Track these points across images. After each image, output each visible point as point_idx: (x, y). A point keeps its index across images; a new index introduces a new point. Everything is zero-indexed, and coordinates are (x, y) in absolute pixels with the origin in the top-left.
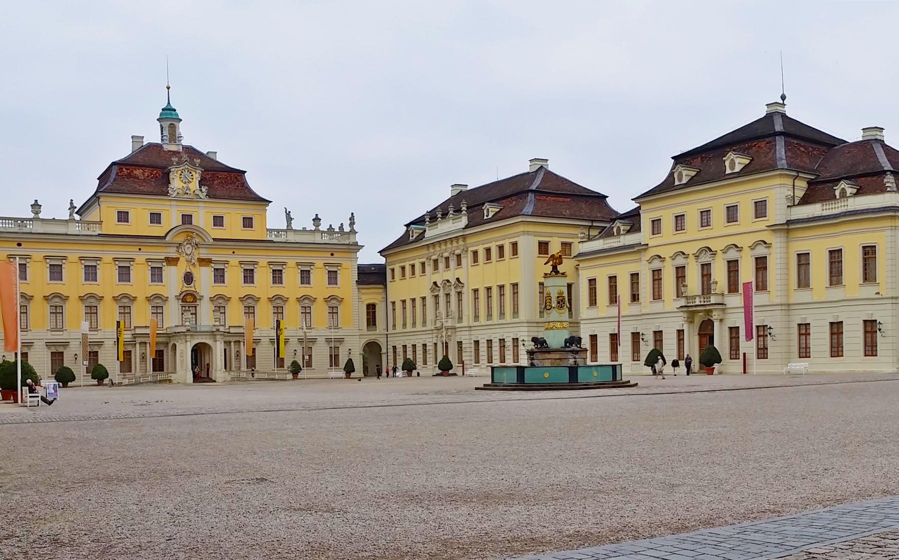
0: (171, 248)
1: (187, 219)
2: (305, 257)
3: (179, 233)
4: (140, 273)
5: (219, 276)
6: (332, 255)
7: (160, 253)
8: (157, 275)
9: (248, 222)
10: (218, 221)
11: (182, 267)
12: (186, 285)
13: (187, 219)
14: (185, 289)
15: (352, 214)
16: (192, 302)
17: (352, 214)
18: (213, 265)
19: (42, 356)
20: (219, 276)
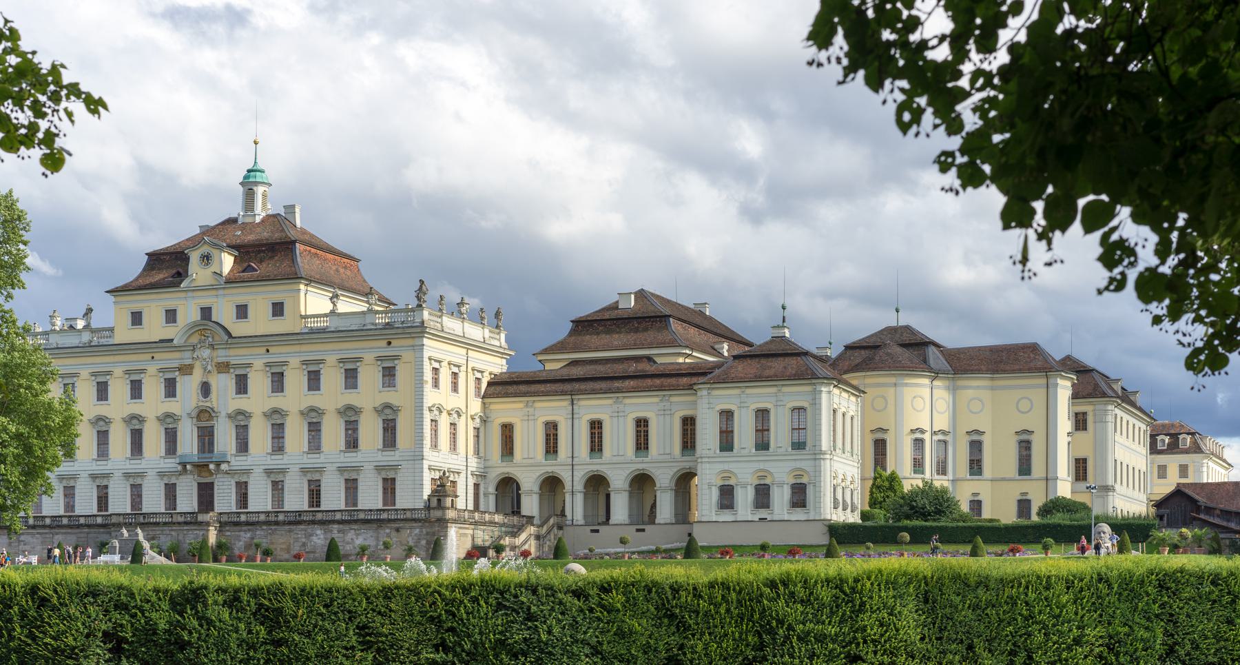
0: (186, 353)
1: (206, 312)
2: (350, 349)
3: (192, 333)
4: (153, 388)
5: (242, 386)
6: (389, 343)
7: (172, 359)
8: (171, 389)
9: (278, 309)
10: (242, 311)
11: (197, 377)
12: (201, 398)
13: (206, 312)
14: (201, 404)
15: (422, 282)
16: (207, 421)
17: (422, 282)
18: (232, 370)
19: (221, 487)
20: (242, 386)
